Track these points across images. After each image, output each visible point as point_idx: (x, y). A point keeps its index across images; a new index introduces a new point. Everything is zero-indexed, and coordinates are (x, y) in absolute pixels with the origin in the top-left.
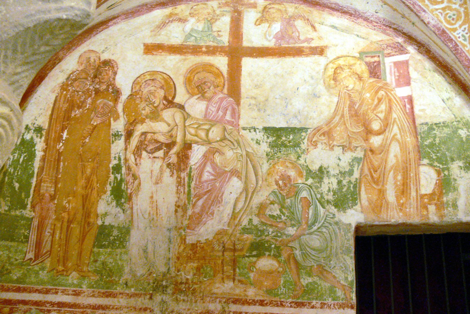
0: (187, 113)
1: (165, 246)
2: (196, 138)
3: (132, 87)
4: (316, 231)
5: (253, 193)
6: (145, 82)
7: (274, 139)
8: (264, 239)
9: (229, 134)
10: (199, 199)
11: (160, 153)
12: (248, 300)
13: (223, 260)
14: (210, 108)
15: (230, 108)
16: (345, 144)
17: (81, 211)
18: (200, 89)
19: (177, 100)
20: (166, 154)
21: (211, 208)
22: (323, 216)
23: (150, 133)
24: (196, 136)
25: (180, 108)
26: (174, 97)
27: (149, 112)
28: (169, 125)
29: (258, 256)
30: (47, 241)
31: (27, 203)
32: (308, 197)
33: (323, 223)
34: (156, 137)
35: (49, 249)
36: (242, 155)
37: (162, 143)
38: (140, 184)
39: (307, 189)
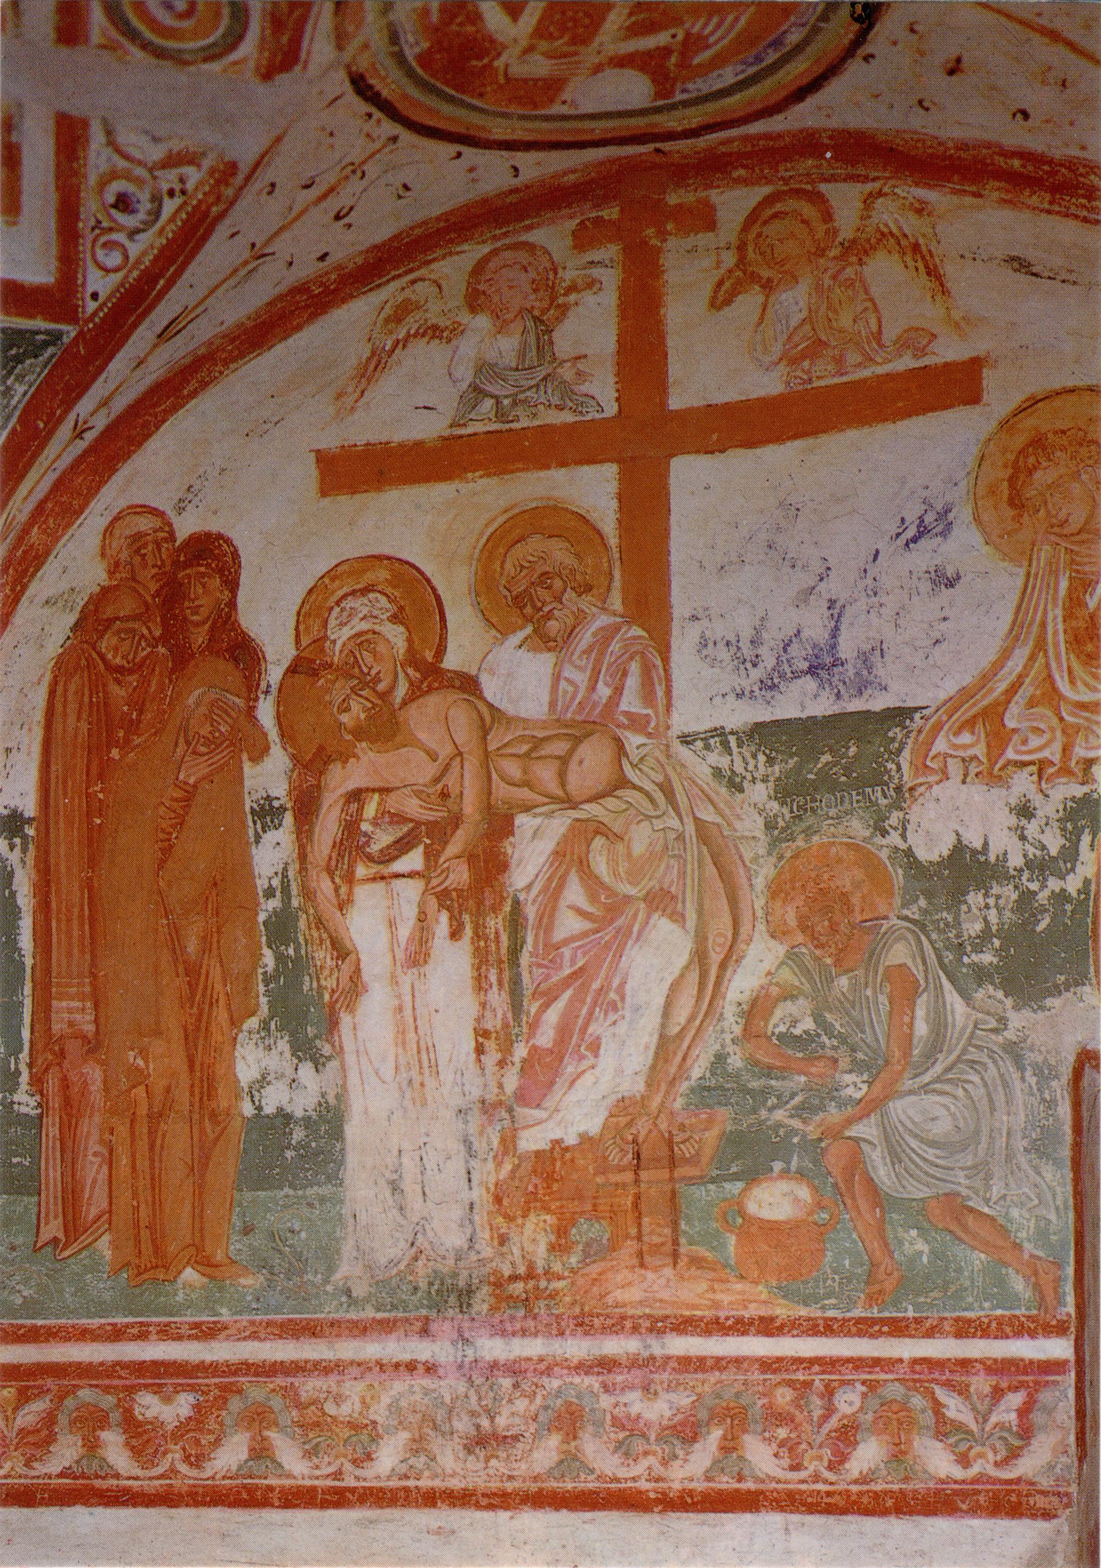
0: (491, 706)
1: (456, 1167)
2: (525, 793)
3: (297, 629)
4: (938, 1080)
5: (723, 966)
6: (338, 603)
7: (792, 762)
8: (768, 1119)
9: (634, 766)
10: (547, 1005)
11: (413, 860)
12: (722, 1320)
13: (638, 1197)
14: (566, 674)
15: (635, 667)
16: (1046, 754)
17: (184, 1078)
18: (528, 610)
19: (451, 661)
20: (431, 856)
21: (590, 1030)
22: (964, 1028)
23: (373, 790)
24: (527, 784)
25: (462, 689)
26: (441, 651)
27: (363, 716)
28: (433, 757)
29: (753, 1176)
30: (95, 1181)
31: (17, 1069)
32: (910, 963)
33: (964, 1051)
34: (393, 802)
35: (105, 1205)
36: (680, 837)
37: (418, 824)
38: (358, 971)
39: (910, 936)
